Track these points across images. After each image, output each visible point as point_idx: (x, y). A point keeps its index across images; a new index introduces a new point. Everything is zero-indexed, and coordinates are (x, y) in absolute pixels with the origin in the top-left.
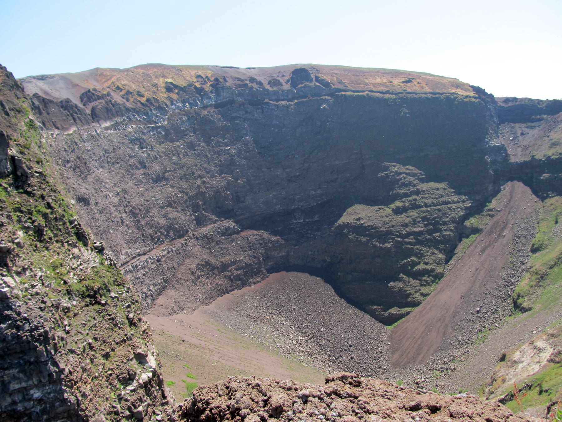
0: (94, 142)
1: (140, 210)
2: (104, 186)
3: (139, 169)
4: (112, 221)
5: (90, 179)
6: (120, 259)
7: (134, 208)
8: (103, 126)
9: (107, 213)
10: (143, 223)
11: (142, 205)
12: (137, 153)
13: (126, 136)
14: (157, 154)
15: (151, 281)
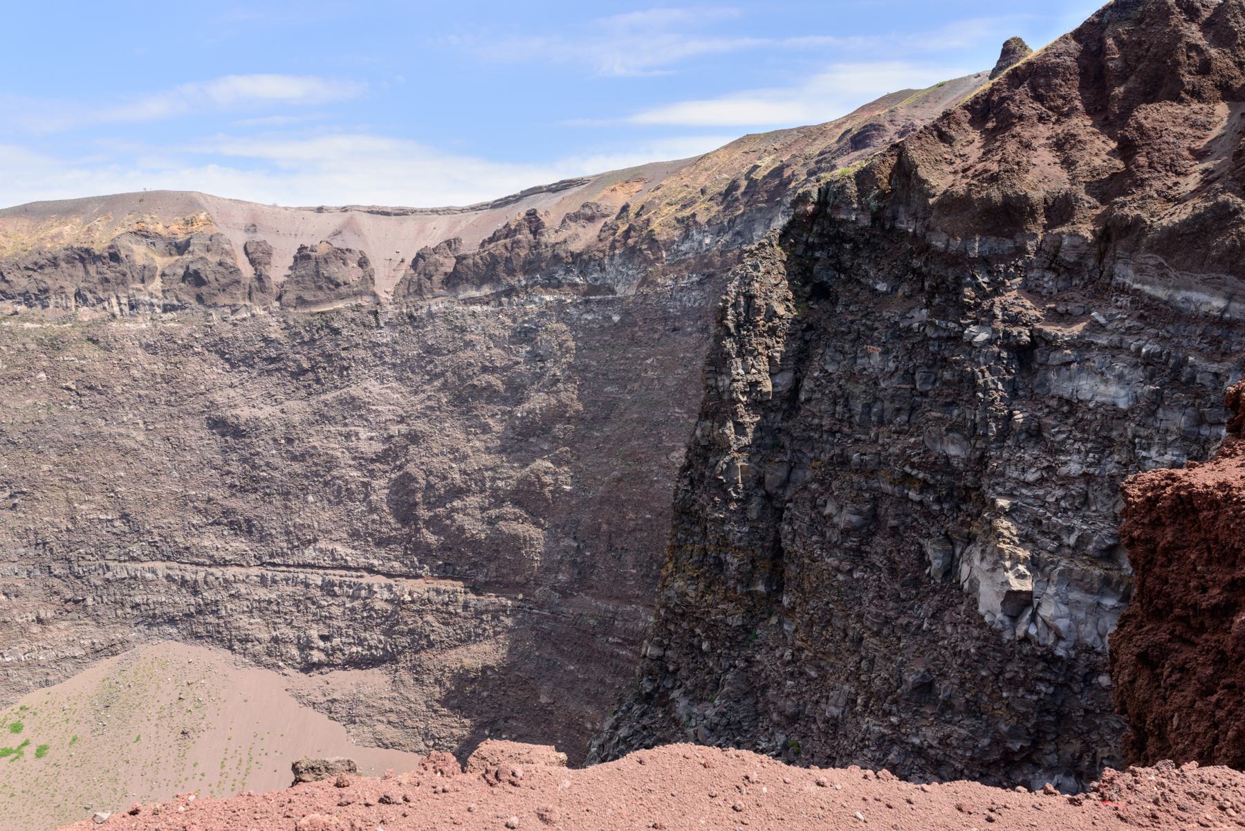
0: (410, 329)
1: (430, 486)
2: (361, 416)
3: (505, 401)
4: (326, 484)
5: (329, 397)
6: (303, 553)
7: (411, 478)
8: (461, 296)
9: (316, 464)
10: (423, 513)
11: (445, 478)
12: (518, 363)
13: (514, 321)
14: (564, 371)
15: (354, 629)
